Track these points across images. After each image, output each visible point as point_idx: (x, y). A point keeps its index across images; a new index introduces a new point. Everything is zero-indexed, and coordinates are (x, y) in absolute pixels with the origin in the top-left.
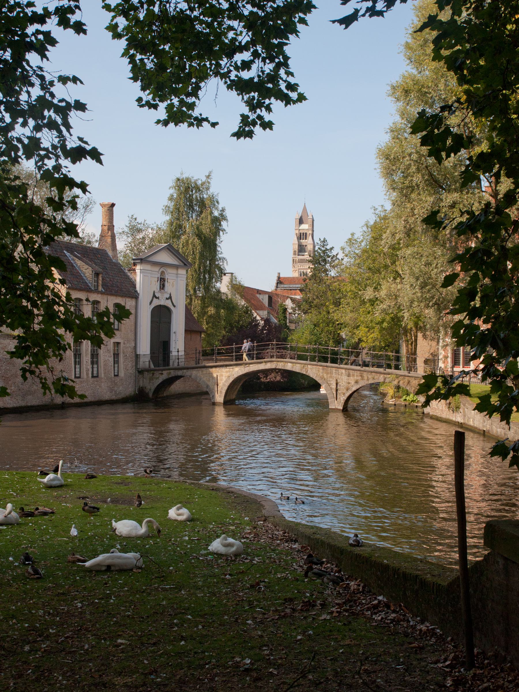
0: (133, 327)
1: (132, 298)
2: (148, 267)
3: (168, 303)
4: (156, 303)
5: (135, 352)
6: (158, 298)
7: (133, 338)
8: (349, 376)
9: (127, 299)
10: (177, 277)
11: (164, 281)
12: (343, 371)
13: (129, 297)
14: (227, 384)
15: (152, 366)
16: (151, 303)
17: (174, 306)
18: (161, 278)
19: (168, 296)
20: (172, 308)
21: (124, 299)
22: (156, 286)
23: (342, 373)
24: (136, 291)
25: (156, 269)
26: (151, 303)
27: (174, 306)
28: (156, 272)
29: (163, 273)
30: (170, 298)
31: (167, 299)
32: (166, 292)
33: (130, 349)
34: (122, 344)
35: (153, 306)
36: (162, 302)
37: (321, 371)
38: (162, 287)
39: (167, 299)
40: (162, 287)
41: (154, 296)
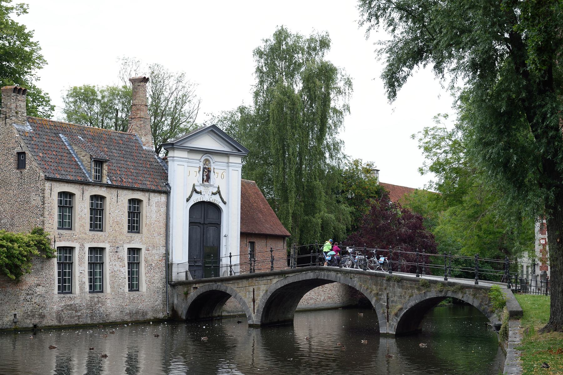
0: (163, 230)
1: (160, 192)
2: (184, 154)
3: (216, 199)
4: (196, 198)
5: (167, 259)
7: (163, 242)
9: (152, 195)
11: (209, 171)
13: (154, 191)
14: (264, 301)
15: (191, 279)
16: (188, 200)
17: (225, 203)
18: (204, 168)
19: (215, 190)
20: (221, 205)
21: (147, 194)
22: (197, 178)
24: (168, 184)
25: (198, 157)
26: (188, 200)
27: (225, 203)
28: (198, 161)
29: (207, 160)
30: (219, 192)
31: (213, 194)
32: (211, 186)
33: (157, 257)
34: (143, 252)
35: (192, 202)
39: (213, 194)
41: (194, 190)
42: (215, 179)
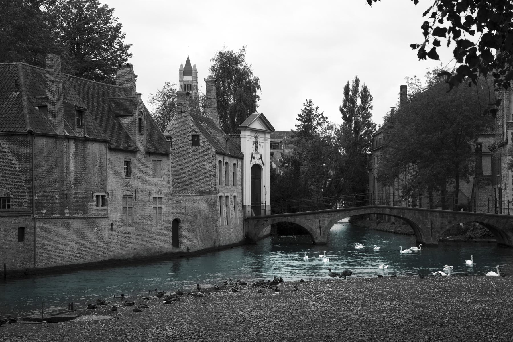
4: (254, 162)
6: (254, 158)
8: (443, 217)
10: (265, 140)
12: (438, 214)
17: (264, 165)
20: (262, 166)
23: (436, 215)
25: (253, 134)
27: (264, 165)
30: (261, 158)
31: (259, 159)
36: (257, 161)
37: (417, 214)
38: (256, 149)
40: (256, 149)
42: (260, 150)
